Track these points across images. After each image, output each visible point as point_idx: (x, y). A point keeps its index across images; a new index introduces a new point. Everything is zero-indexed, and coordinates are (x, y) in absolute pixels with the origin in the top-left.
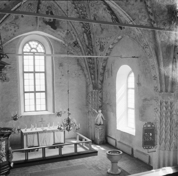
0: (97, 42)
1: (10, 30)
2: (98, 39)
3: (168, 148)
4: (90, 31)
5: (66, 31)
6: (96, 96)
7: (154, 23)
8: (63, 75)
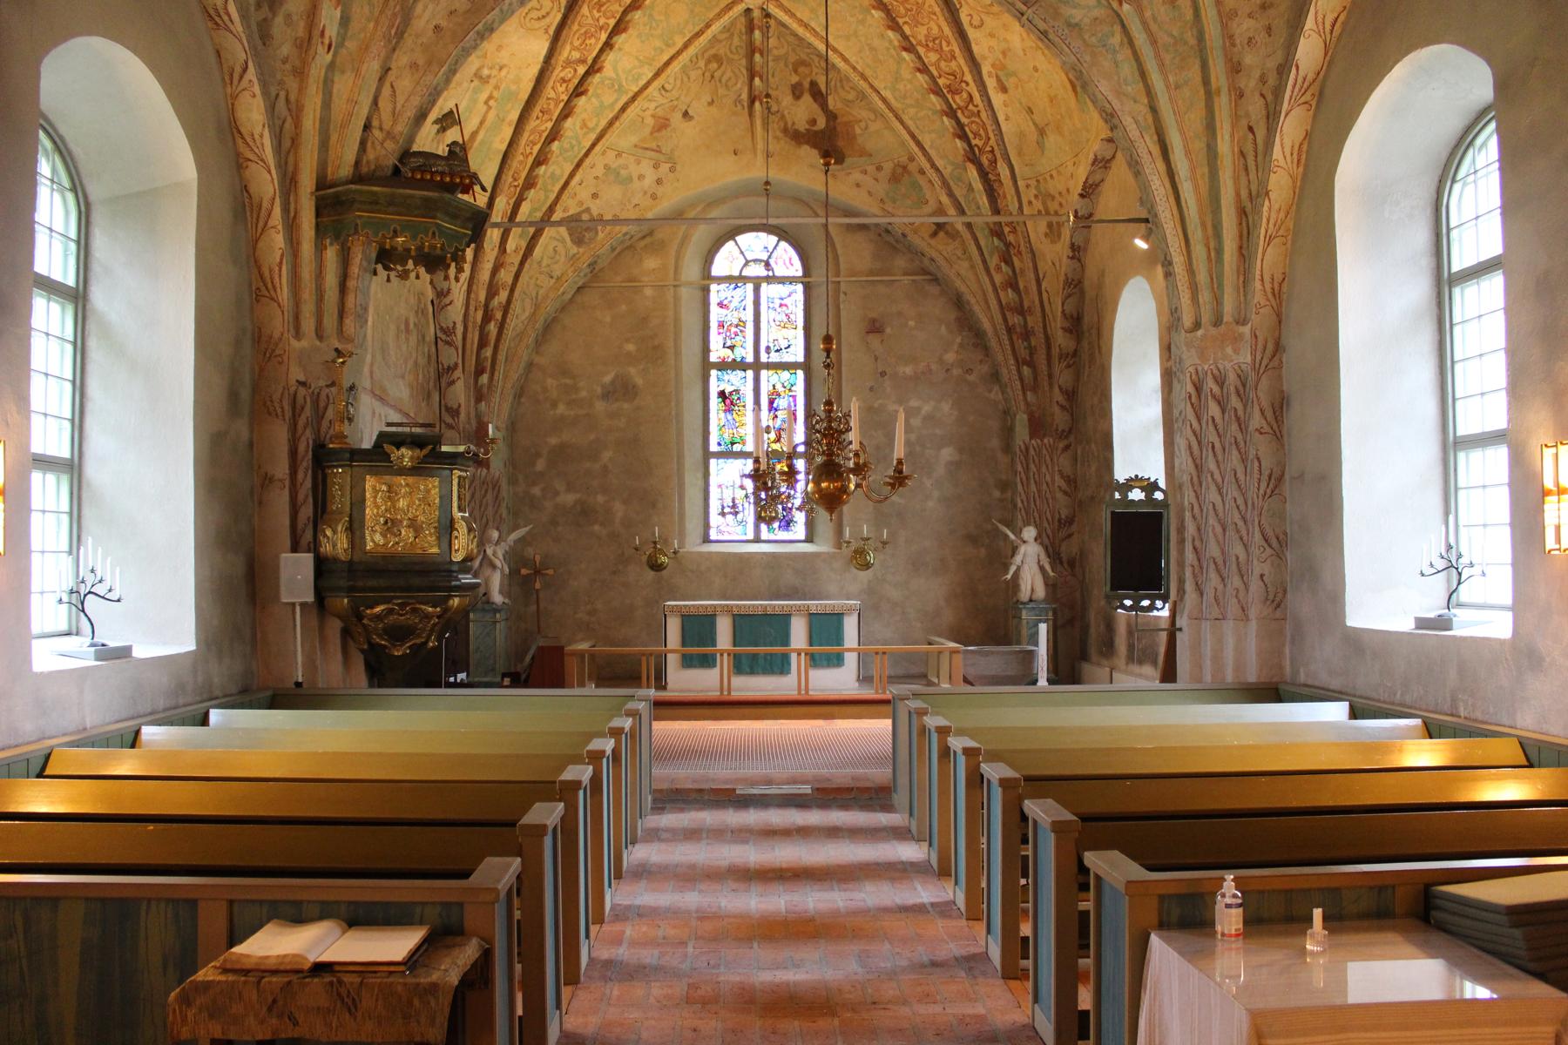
0: (1030, 203)
2: (1033, 183)
3: (1233, 608)
4: (992, 151)
5: (888, 166)
8: (883, 374)
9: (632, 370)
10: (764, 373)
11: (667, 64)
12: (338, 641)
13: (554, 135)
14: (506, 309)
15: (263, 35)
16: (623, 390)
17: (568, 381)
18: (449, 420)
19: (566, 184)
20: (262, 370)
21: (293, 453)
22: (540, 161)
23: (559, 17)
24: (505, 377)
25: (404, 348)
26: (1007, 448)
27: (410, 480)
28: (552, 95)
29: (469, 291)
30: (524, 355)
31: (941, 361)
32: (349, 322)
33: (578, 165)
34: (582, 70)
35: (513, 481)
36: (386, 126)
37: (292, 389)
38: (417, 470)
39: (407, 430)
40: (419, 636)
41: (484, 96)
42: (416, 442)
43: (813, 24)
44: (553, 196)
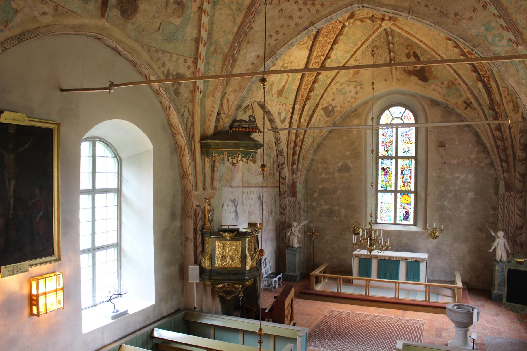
0: (505, 97)
1: (348, 92)
2: (506, 90)
4: (488, 76)
5: (446, 83)
6: (511, 205)
7: (517, 46)
8: (445, 163)
9: (349, 162)
10: (399, 161)
11: (356, 52)
13: (315, 82)
14: (302, 141)
15: (177, 93)
16: (345, 168)
17: (326, 165)
18: (282, 181)
19: (322, 97)
20: (185, 202)
22: (311, 91)
23: (311, 42)
24: (303, 165)
26: (497, 193)
27: (231, 242)
29: (288, 137)
30: (310, 157)
31: (469, 158)
33: (326, 90)
34: (323, 58)
35: (306, 200)
36: (226, 113)
37: (194, 209)
38: (233, 239)
43: (411, 32)
44: (317, 101)
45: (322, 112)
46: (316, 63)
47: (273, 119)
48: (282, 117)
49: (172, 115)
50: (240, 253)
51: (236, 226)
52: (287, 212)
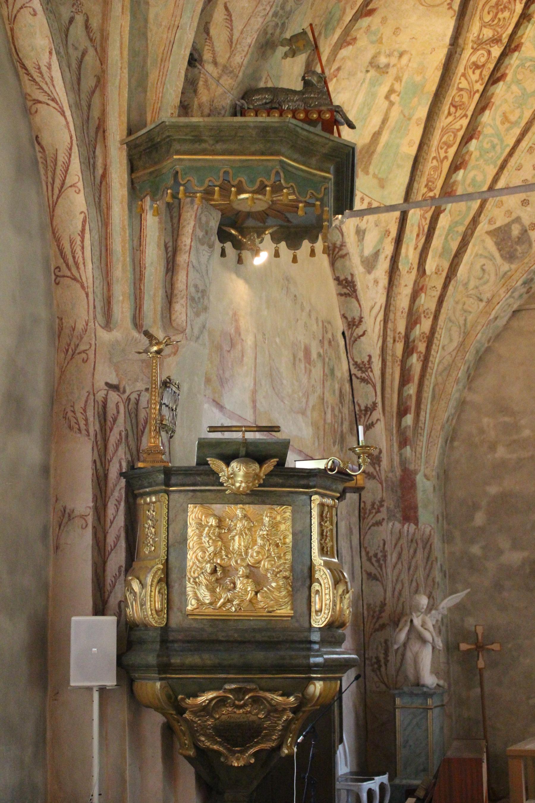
12: (158, 743)
17: (507, 419)
21: (101, 482)
24: (433, 418)
25: (305, 380)
27: (251, 509)
28: (464, 84)
29: (386, 321)
30: (454, 391)
32: (181, 311)
33: (502, 167)
34: (496, 51)
35: (447, 538)
36: (221, 60)
37: (100, 395)
38: (257, 495)
39: (237, 436)
40: (267, 738)
41: (384, 90)
42: (255, 454)
45: (490, 244)
46: (476, 66)
47: (343, 245)
48: (368, 251)
49: (25, 18)
50: (289, 556)
51: (275, 429)
52: (390, 574)
